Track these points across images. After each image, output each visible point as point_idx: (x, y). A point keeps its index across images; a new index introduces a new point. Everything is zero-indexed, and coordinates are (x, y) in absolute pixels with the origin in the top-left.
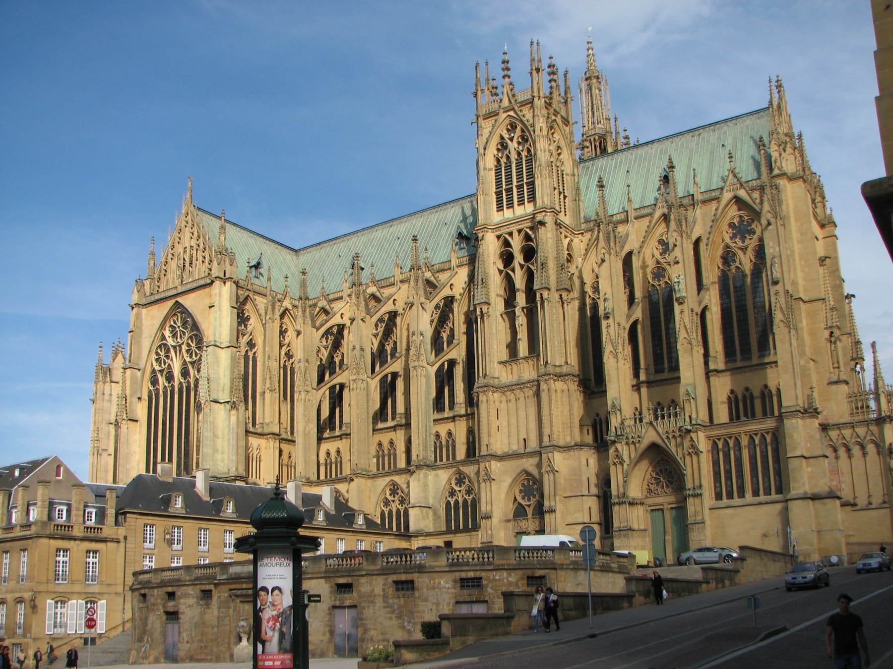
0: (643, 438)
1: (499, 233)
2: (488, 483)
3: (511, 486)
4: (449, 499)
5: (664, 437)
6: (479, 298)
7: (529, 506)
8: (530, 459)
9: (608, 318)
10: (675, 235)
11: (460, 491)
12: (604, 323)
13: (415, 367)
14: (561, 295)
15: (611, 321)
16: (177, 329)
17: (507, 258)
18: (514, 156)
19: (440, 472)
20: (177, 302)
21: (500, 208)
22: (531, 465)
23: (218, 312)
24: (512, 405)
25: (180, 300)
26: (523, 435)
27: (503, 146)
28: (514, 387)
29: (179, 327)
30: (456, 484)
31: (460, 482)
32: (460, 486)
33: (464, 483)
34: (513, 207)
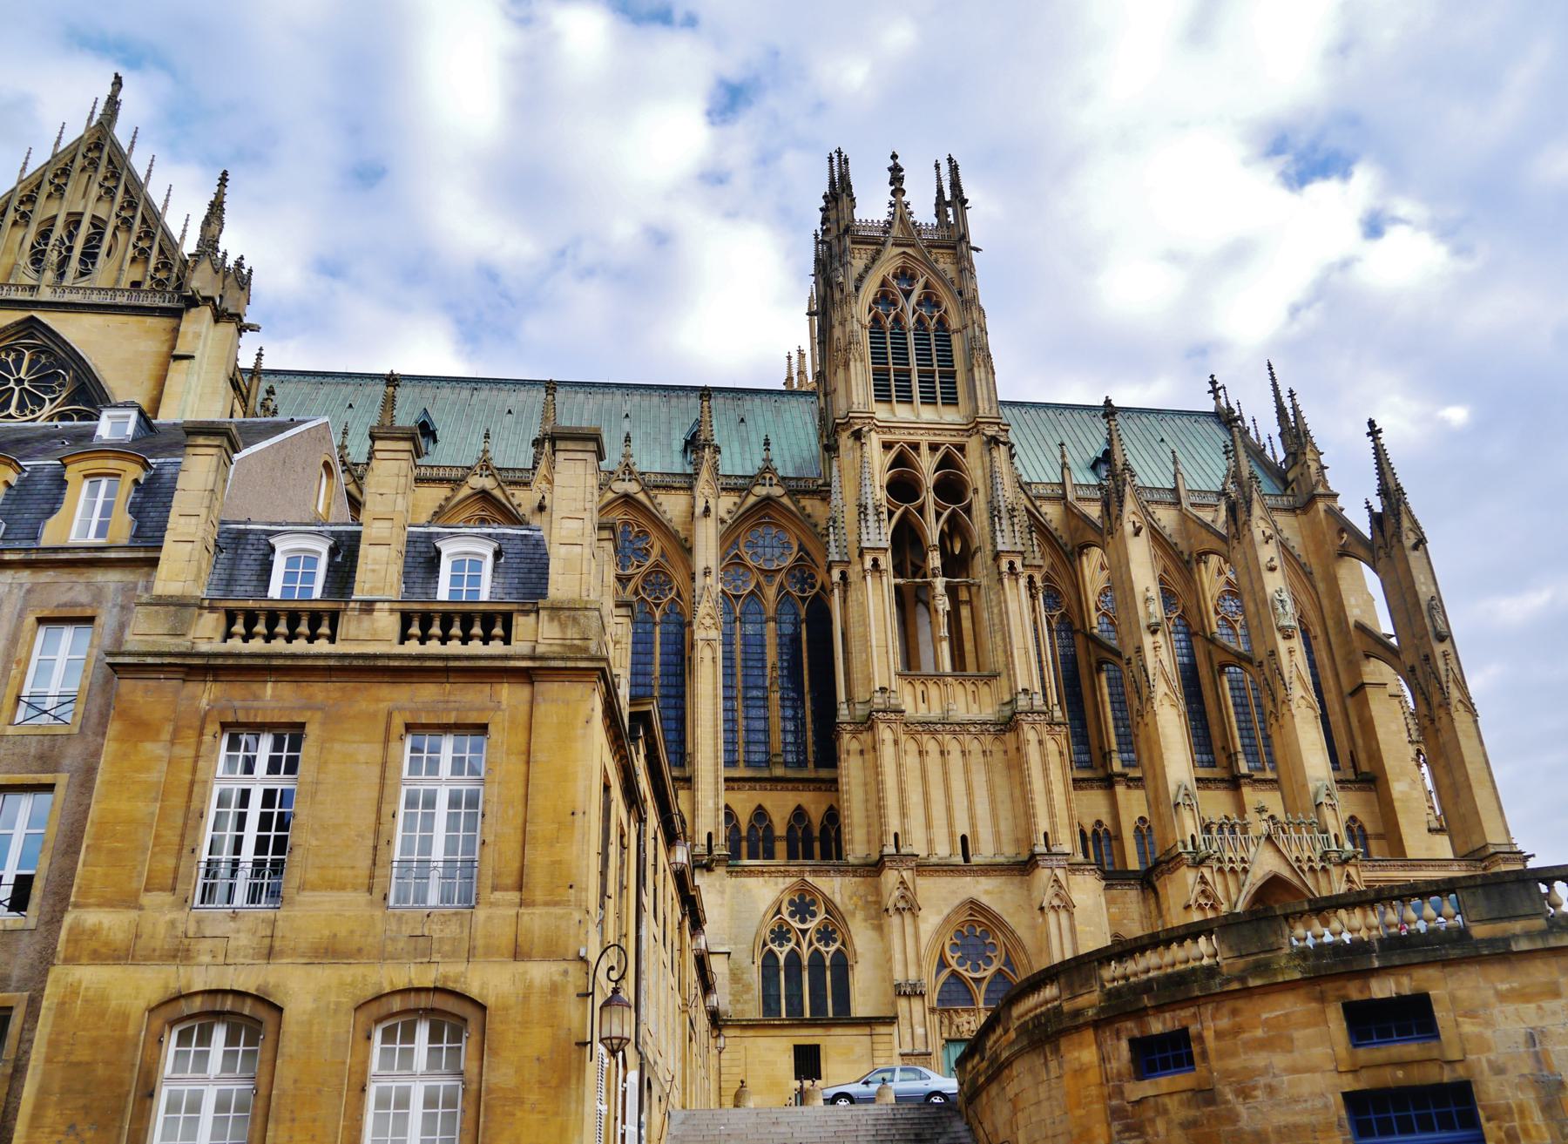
0: (1252, 863)
1: (888, 437)
2: (907, 915)
3: (939, 932)
4: (771, 946)
5: (1295, 866)
6: (871, 537)
7: (978, 981)
8: (983, 880)
9: (1154, 632)
10: (1263, 525)
11: (804, 932)
12: (1148, 641)
13: (708, 642)
14: (1031, 578)
15: (1159, 637)
16: (12, 384)
17: (903, 487)
18: (910, 321)
19: (751, 882)
20: (32, 318)
21: (883, 395)
22: (986, 892)
23: (196, 377)
24: (933, 757)
25: (44, 317)
26: (962, 828)
27: (884, 297)
28: (939, 727)
29: (19, 381)
30: (792, 915)
31: (802, 908)
32: (803, 921)
33: (814, 915)
34: (911, 402)
